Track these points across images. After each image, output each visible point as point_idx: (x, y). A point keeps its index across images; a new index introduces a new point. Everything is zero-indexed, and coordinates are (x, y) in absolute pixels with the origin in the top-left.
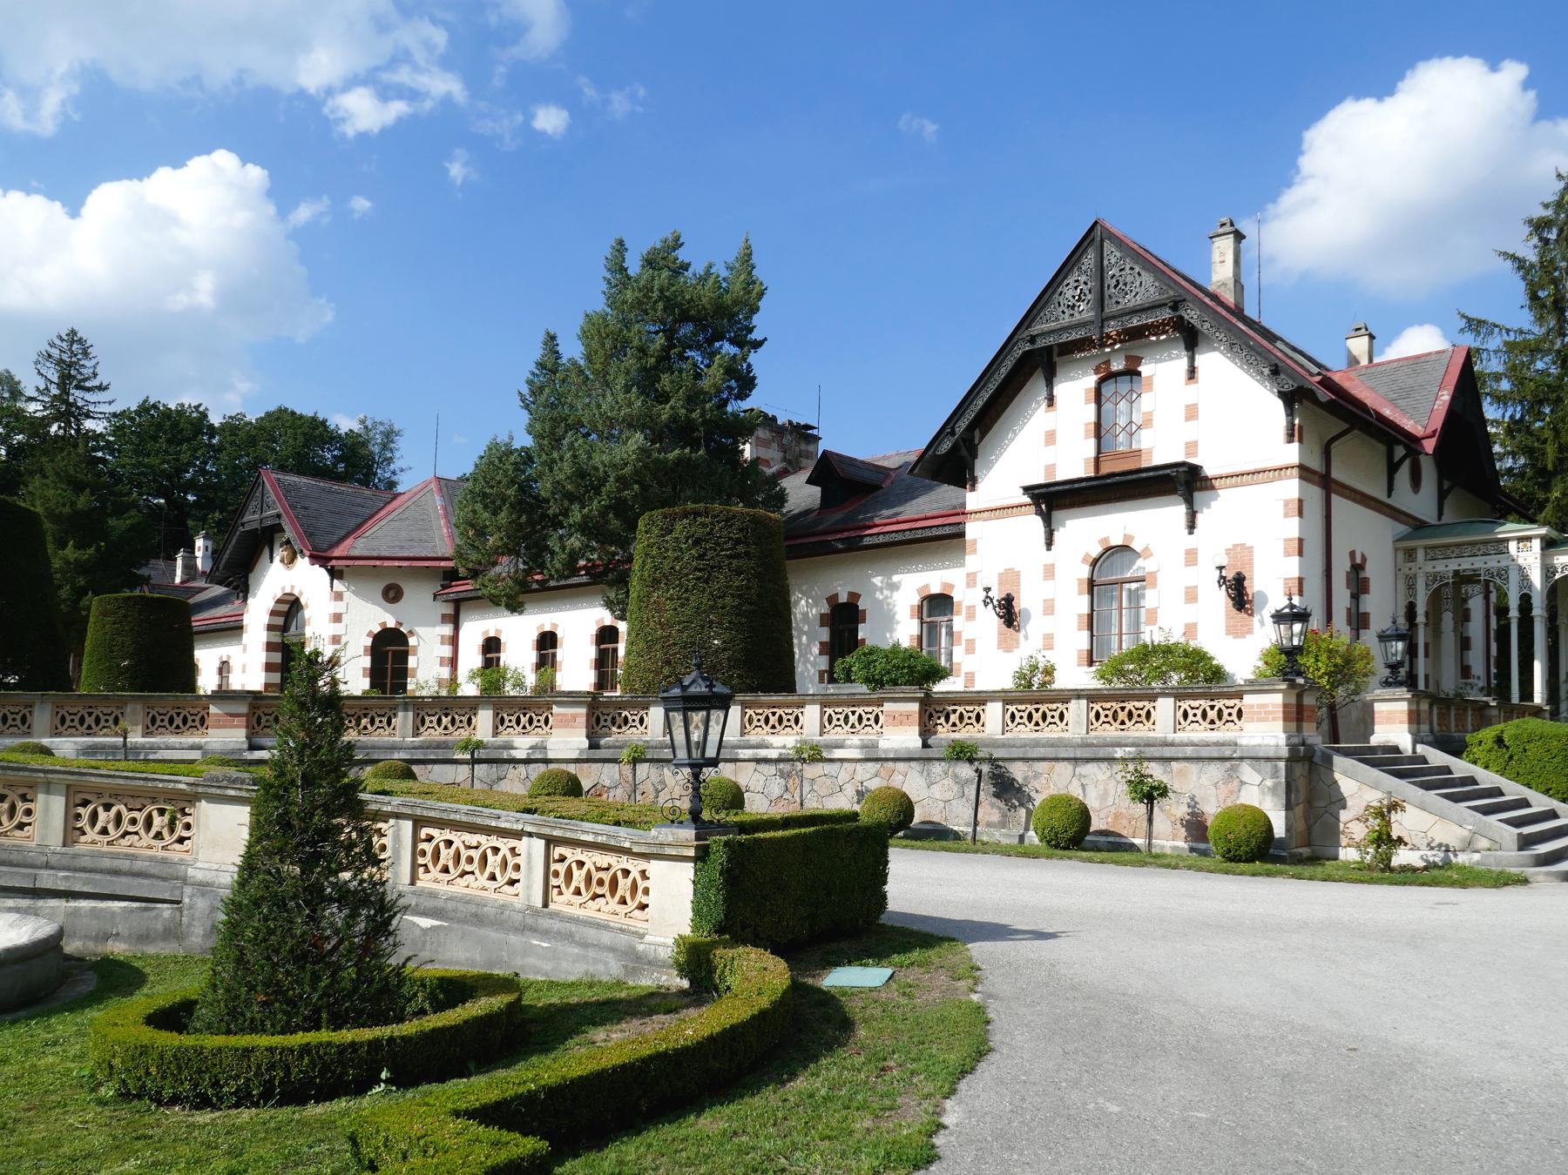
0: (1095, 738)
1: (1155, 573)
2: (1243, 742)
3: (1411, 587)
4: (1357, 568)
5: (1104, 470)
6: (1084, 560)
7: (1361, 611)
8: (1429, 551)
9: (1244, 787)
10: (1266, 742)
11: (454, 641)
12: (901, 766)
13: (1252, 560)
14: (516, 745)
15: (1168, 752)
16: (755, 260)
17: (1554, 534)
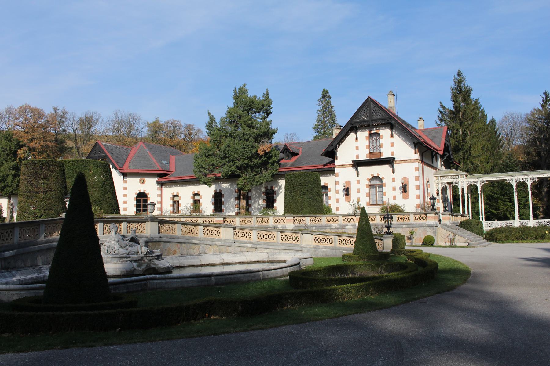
6: (367, 179)
11: (161, 196)
14: (278, 226)
15: (413, 226)
16: (269, 92)
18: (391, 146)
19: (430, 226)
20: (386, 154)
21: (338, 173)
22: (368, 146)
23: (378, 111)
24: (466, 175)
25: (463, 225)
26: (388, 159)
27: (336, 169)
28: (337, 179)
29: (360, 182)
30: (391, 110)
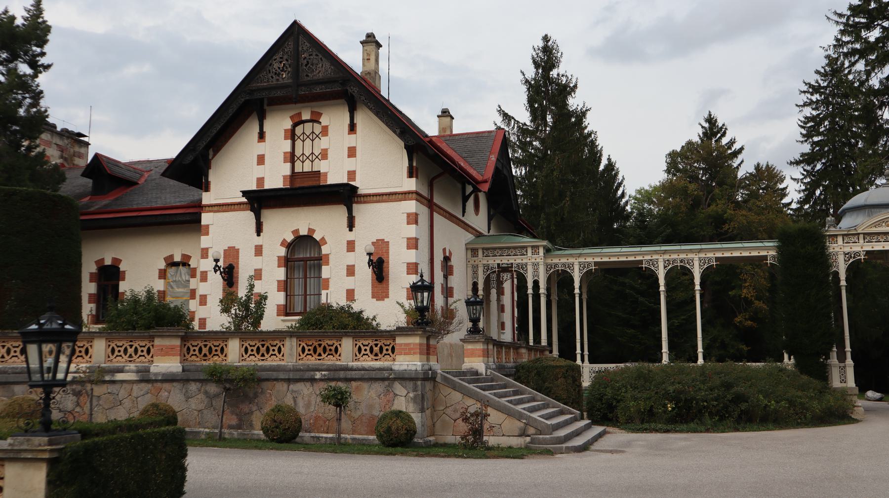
0: (302, 365)
1: (328, 255)
2: (396, 368)
3: (475, 273)
4: (447, 259)
5: (298, 185)
6: (282, 244)
7: (449, 286)
8: (485, 251)
9: (396, 398)
10: (410, 368)
12: (166, 386)
13: (388, 250)
17: (550, 246)
18: (349, 156)
19: (404, 378)
20: (335, 175)
21: (207, 226)
22: (289, 155)
23: (315, 61)
24: (544, 247)
25: (520, 374)
26: (336, 189)
27: (204, 215)
28: (205, 242)
29: (265, 251)
30: (368, 78)
